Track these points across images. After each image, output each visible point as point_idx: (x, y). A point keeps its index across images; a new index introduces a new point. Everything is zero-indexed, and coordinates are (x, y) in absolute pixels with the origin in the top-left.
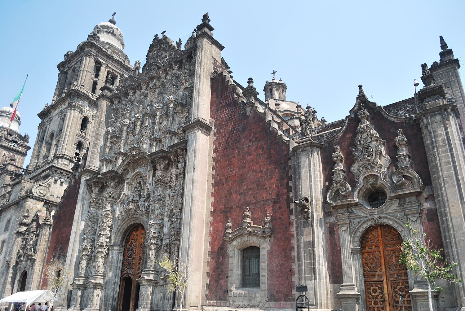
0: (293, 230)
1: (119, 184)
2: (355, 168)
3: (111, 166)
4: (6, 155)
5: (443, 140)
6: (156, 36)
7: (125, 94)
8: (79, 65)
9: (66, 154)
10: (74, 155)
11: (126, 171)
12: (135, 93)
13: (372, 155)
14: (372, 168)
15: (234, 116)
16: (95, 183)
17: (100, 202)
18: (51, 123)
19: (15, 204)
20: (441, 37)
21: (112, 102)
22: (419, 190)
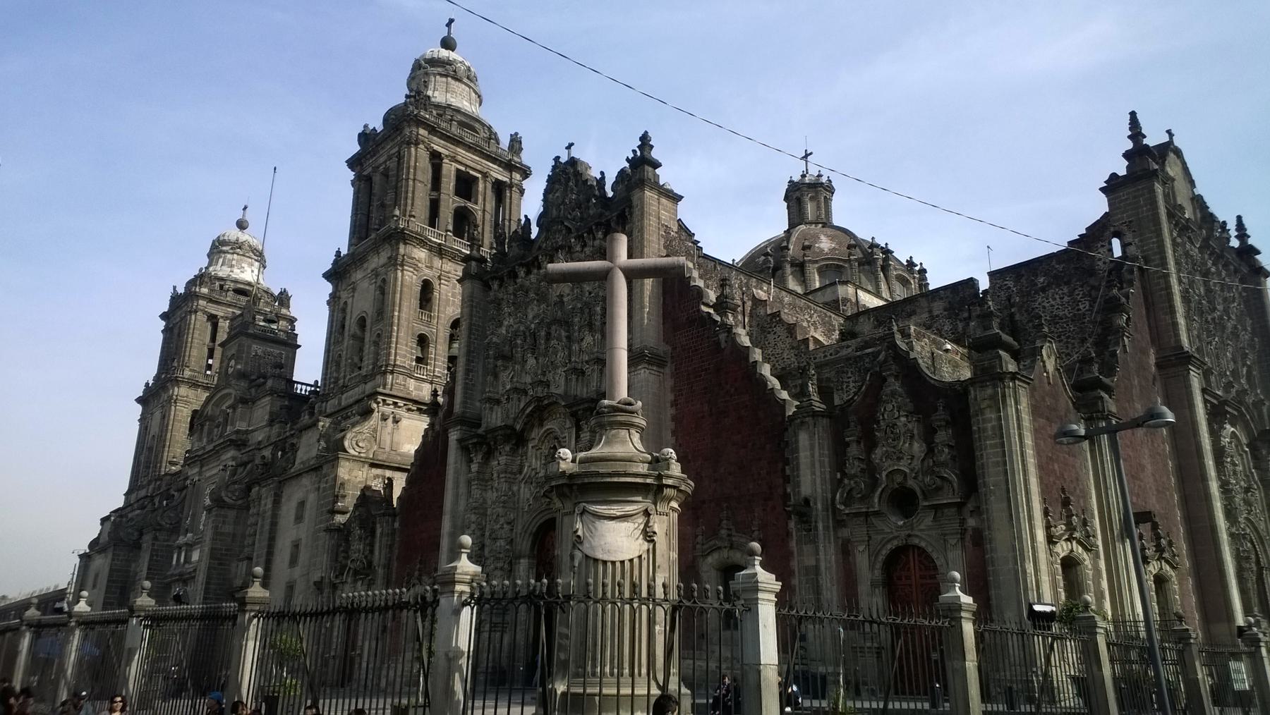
0: (793, 544)
1: (518, 447)
2: (878, 452)
3: (500, 410)
4: (259, 352)
5: (993, 427)
6: (557, 159)
7: (509, 272)
8: (396, 163)
9: (398, 363)
10: (414, 363)
11: (529, 426)
12: (528, 273)
13: (899, 438)
14: (899, 459)
15: (701, 344)
16: (474, 444)
17: (487, 476)
18: (356, 295)
19: (312, 470)
20: (1133, 115)
21: (487, 287)
22: (959, 500)
